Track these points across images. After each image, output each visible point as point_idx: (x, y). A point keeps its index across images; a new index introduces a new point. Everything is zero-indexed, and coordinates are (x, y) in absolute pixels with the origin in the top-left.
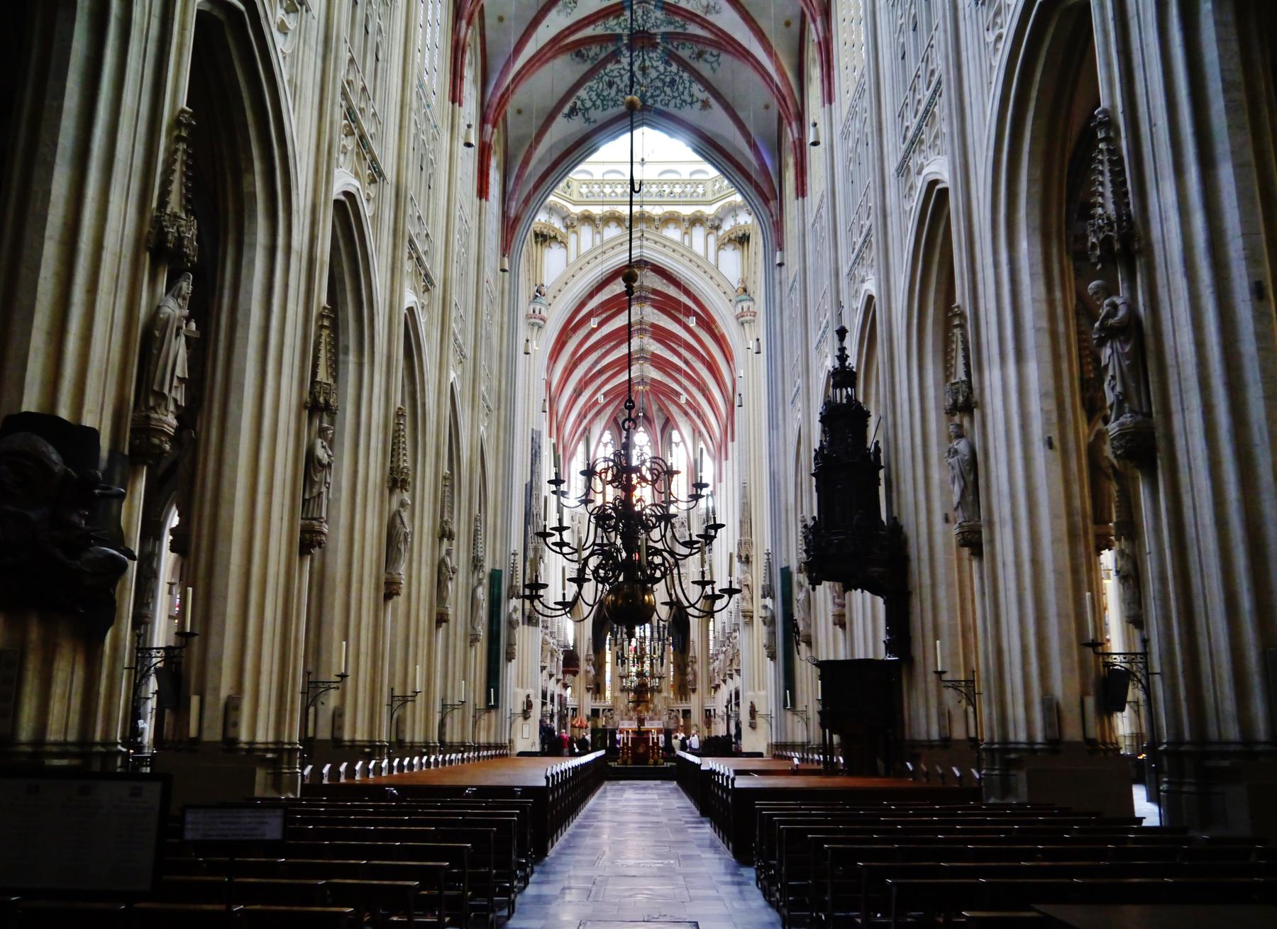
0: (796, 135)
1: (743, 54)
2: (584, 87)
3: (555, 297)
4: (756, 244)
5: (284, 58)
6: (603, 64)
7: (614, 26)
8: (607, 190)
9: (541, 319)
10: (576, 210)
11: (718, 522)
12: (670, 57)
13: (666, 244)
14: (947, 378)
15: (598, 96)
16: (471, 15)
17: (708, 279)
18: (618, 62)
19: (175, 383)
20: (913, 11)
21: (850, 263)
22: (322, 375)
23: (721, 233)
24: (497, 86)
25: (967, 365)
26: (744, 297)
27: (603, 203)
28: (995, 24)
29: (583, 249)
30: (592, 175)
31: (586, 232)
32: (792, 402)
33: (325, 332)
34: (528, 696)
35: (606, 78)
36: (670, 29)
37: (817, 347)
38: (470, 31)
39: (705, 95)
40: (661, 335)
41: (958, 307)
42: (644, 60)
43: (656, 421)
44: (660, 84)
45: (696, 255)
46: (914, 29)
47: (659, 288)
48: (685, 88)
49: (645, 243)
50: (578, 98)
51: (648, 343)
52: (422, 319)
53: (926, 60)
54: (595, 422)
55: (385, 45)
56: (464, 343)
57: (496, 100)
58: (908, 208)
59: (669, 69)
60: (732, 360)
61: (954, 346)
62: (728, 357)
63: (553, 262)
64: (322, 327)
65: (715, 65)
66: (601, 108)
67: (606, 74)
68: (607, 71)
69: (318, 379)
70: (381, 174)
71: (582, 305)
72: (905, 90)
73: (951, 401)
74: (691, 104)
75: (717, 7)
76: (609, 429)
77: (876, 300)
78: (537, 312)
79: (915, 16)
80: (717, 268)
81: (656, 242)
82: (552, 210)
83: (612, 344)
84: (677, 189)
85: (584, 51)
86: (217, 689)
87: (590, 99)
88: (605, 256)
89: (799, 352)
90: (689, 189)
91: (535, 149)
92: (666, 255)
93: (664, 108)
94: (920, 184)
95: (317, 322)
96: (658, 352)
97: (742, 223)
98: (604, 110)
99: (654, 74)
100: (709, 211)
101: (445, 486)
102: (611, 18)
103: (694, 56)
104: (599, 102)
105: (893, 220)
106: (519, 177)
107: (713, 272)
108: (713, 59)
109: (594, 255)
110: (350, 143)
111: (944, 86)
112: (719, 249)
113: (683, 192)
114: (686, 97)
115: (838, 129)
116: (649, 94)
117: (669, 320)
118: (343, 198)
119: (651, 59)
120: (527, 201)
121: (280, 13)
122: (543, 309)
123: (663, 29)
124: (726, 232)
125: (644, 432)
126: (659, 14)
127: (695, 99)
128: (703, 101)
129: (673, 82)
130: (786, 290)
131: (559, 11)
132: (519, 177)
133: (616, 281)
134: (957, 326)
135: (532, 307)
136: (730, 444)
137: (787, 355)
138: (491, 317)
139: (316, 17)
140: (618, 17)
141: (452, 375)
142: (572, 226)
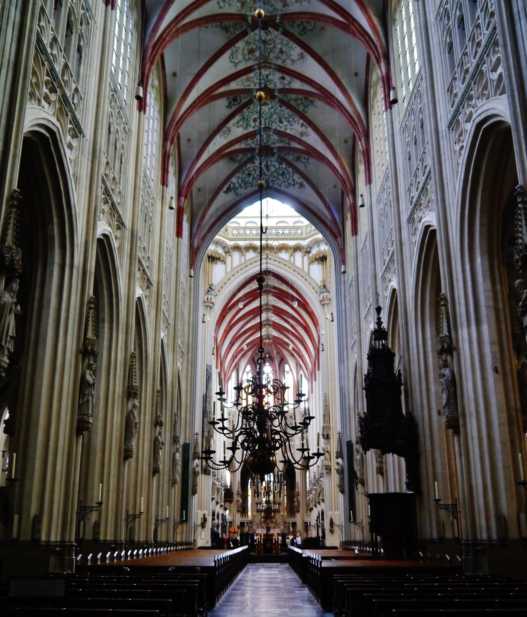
0: (351, 201)
1: (322, 158)
2: (235, 176)
4: (330, 261)
5: (71, 162)
6: (245, 164)
7: (250, 143)
8: (248, 232)
9: (212, 303)
10: (231, 243)
11: (311, 415)
12: (282, 160)
13: (280, 261)
14: (438, 334)
15: (242, 181)
16: (173, 138)
18: (253, 163)
19: (8, 339)
20: (414, 134)
21: (383, 271)
22: (90, 335)
23: (311, 255)
24: (187, 176)
25: (449, 327)
26: (324, 290)
27: (245, 240)
28: (459, 140)
29: (235, 265)
30: (239, 224)
31: (236, 255)
32: (352, 348)
33: (92, 311)
35: (247, 172)
36: (282, 145)
37: (365, 318)
38: (172, 147)
39: (301, 180)
40: (278, 312)
41: (443, 295)
42: (267, 162)
44: (276, 174)
45: (297, 267)
46: (415, 144)
47: (277, 286)
48: (290, 176)
49: (269, 261)
50: (232, 182)
51: (271, 316)
52: (145, 304)
53: (422, 160)
54: (242, 360)
55: (126, 155)
56: (169, 317)
57: (186, 184)
58: (414, 241)
59: (281, 166)
60: (318, 325)
61: (441, 316)
62: (316, 323)
64: (90, 308)
65: (307, 164)
67: (247, 169)
68: (247, 167)
69: (88, 337)
70: (123, 224)
71: (234, 295)
72: (411, 176)
73: (440, 347)
74: (294, 185)
75: (307, 133)
76: (250, 364)
77: (397, 291)
78: (209, 299)
79: (415, 137)
81: (275, 261)
82: (217, 243)
83: (251, 317)
84: (286, 231)
85: (234, 157)
86: (29, 511)
87: (238, 183)
88: (247, 268)
89: (355, 321)
90: (293, 231)
91: (208, 210)
92: (281, 268)
93: (279, 188)
94: (420, 227)
95: (87, 305)
96: (277, 321)
98: (246, 188)
99: (273, 169)
100: (304, 243)
102: (249, 139)
103: (295, 159)
104: (243, 185)
105: (406, 247)
106: (199, 226)
107: (307, 277)
108: (305, 161)
109: (240, 268)
110: (106, 208)
111: (432, 174)
112: (310, 264)
113: (290, 233)
114: (291, 181)
115: (374, 198)
116: (270, 180)
117: (283, 304)
118: (102, 237)
119: (271, 161)
120: (203, 239)
121: (69, 138)
122: (213, 298)
123: (278, 145)
124: (313, 255)
125: (270, 365)
126: (275, 137)
127: (296, 183)
128: (300, 184)
129: (283, 174)
130: (347, 286)
131: (221, 136)
132: (199, 226)
133: (253, 282)
134: (442, 305)
135: (206, 297)
136: (317, 372)
137: (348, 322)
138: (184, 302)
139: (88, 140)
140: (253, 139)
142: (229, 252)
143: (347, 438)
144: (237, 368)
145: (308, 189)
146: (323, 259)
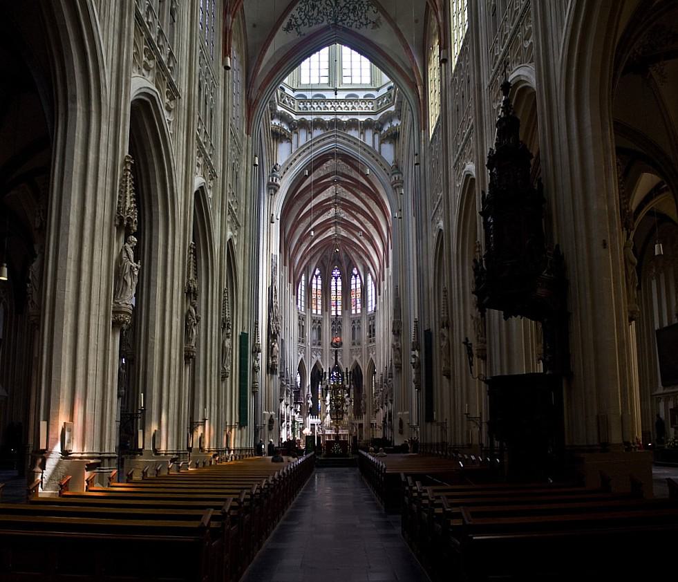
3: (284, 173)
17: (374, 161)
23: (382, 132)
26: (396, 171)
27: (311, 114)
29: (301, 144)
34: (272, 416)
43: (344, 263)
44: (347, 11)
45: (368, 146)
47: (346, 173)
63: (283, 153)
66: (308, 25)
74: (367, 24)
80: (380, 153)
81: (344, 139)
82: (283, 117)
96: (345, 218)
97: (395, 125)
101: (191, 253)
107: (377, 156)
114: (363, 20)
116: (339, 19)
117: (353, 196)
127: (369, 21)
133: (321, 168)
141: (229, 234)
143: (424, 326)
144: (307, 269)
145: (386, 26)
146: (393, 137)
